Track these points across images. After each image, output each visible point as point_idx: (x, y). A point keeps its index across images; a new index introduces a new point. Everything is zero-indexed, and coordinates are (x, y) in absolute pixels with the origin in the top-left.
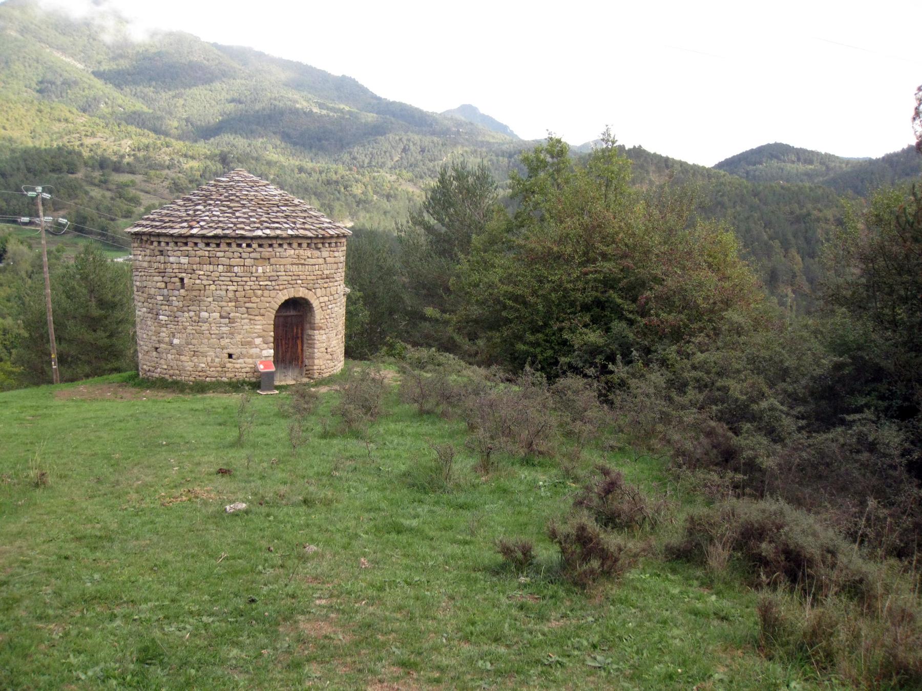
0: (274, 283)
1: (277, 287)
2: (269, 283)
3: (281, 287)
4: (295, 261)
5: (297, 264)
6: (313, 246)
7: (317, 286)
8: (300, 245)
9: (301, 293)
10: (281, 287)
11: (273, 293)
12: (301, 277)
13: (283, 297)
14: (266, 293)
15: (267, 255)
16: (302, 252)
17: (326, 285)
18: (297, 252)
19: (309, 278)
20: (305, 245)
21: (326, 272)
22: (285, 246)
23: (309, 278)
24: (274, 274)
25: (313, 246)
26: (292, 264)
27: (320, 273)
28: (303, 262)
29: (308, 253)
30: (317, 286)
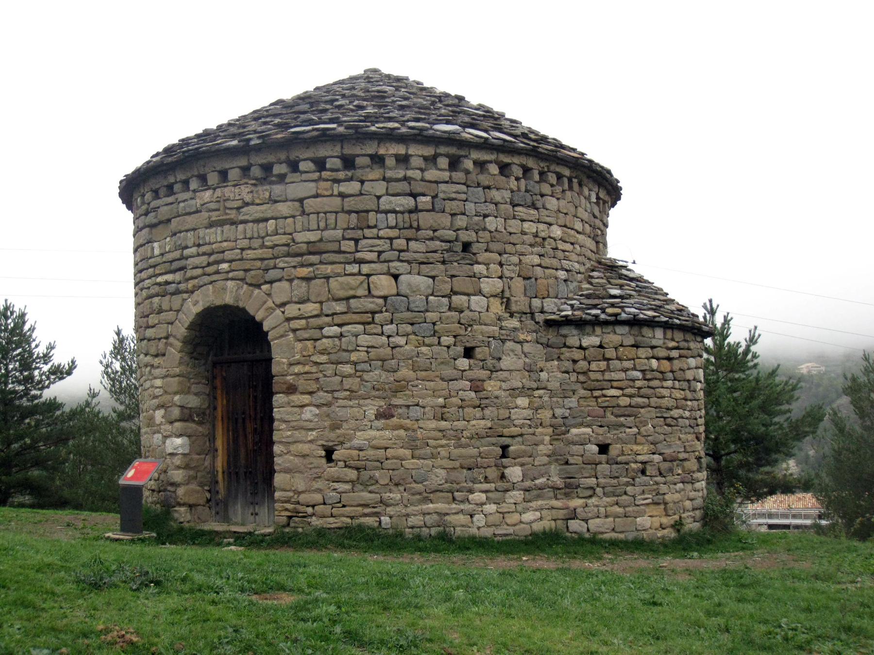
0: (178, 276)
1: (182, 286)
2: (169, 277)
3: (190, 285)
4: (215, 217)
5: (221, 223)
6: (256, 172)
7: (272, 274)
8: (224, 175)
9: (229, 293)
10: (190, 285)
11: (177, 300)
12: (228, 255)
13: (194, 306)
14: (166, 302)
15: (164, 212)
16: (228, 191)
17: (304, 272)
18: (219, 192)
19: (250, 254)
20: (234, 174)
21: (300, 237)
22: (194, 185)
23: (250, 254)
24: (177, 254)
25: (256, 172)
26: (211, 225)
27: (284, 239)
28: (233, 214)
29: (245, 192)
30: (272, 274)
